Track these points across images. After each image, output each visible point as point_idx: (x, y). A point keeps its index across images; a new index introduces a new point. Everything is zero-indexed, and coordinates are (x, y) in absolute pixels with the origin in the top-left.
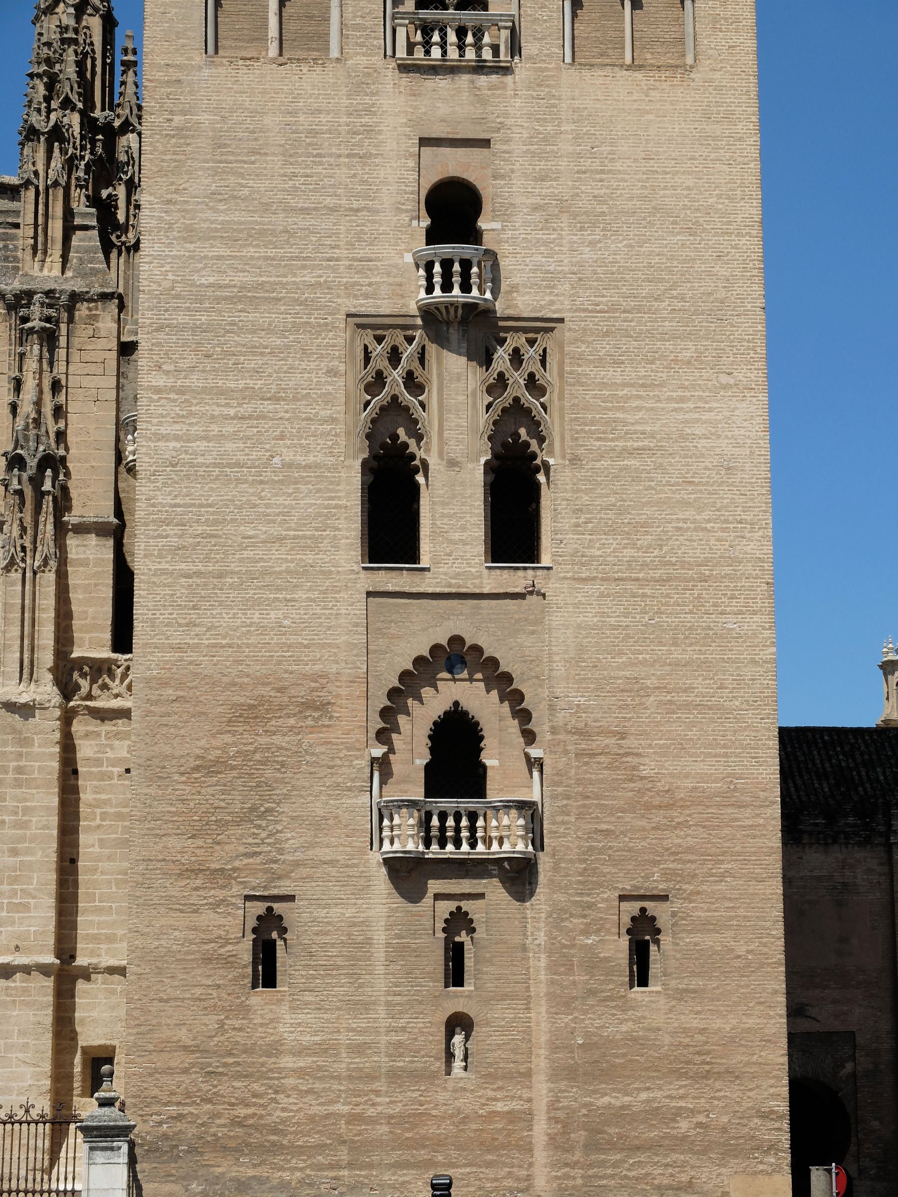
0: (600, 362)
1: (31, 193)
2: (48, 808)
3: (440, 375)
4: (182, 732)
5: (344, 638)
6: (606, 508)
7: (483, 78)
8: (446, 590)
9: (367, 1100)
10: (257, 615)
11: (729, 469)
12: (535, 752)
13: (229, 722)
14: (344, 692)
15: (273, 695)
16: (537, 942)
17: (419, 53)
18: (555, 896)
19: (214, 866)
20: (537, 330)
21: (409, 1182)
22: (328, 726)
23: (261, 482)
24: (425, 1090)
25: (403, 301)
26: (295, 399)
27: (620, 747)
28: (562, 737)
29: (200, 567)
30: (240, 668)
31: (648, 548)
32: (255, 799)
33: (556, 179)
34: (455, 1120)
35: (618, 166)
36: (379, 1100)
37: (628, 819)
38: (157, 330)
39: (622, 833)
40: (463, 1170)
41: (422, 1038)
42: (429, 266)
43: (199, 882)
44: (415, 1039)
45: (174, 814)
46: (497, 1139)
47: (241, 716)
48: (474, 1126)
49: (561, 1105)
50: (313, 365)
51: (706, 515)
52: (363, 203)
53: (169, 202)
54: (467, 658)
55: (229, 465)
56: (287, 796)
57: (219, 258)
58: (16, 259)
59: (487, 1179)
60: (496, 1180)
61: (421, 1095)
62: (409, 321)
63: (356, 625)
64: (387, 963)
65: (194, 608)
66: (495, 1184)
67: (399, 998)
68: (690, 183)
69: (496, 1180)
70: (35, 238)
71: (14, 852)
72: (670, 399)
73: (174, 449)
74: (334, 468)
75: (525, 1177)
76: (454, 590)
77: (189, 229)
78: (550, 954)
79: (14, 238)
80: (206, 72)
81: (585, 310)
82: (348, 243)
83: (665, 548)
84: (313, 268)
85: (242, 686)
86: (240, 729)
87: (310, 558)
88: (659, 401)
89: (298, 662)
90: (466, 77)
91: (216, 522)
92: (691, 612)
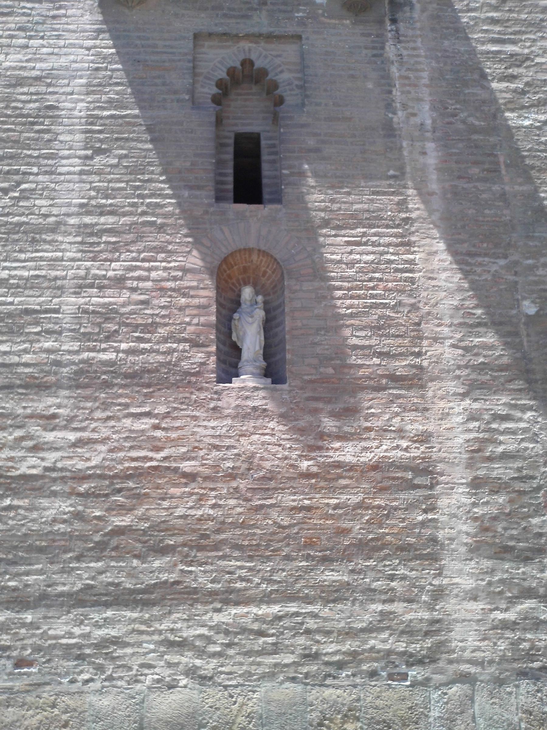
9: (22, 438)
16: (417, 120)
18: (446, 43)
21: (116, 642)
24: (167, 415)
34: (242, 484)
36: (50, 436)
40: (264, 610)
41: (163, 301)
44: (145, 303)
46: (345, 532)
48: (289, 500)
49: (500, 449)
59: (328, 633)
60: (350, 633)
61: (156, 427)
64: (89, 152)
66: (349, 645)
67: (111, 219)
69: (350, 633)
75: (424, 627)
78: (445, 140)
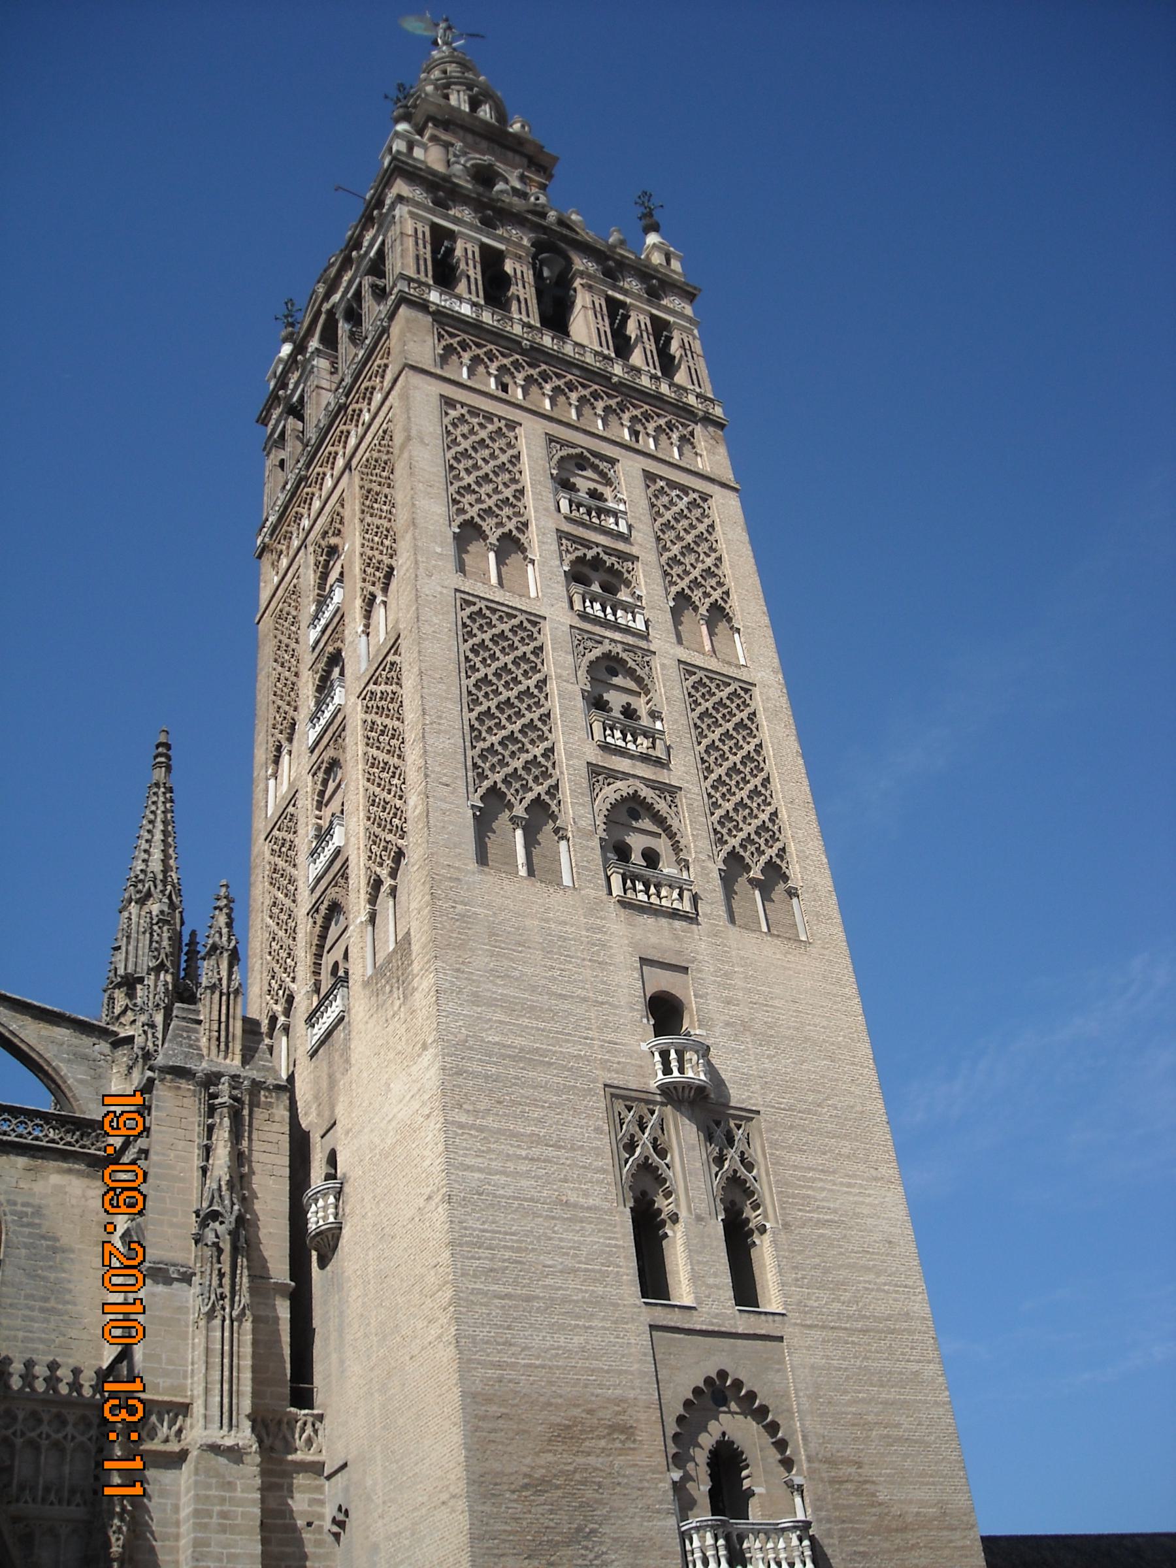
0: (790, 1149)
1: (217, 995)
2: (251, 1556)
3: (679, 1144)
4: (509, 1449)
5: (636, 1366)
6: (815, 1267)
7: (677, 922)
8: (710, 1328)
10: (562, 1340)
11: (890, 1242)
12: (798, 1480)
13: (550, 1440)
14: (643, 1416)
15: (584, 1415)
17: (630, 894)
20: (741, 1118)
22: (634, 1449)
23: (553, 1218)
25: (643, 1080)
26: (573, 1149)
27: (860, 1475)
28: (816, 1465)
30: (554, 1389)
31: (848, 1303)
32: (579, 1520)
33: (738, 1005)
35: (776, 1003)
37: (876, 1542)
38: (456, 1073)
39: (876, 1554)
42: (665, 1055)
45: (510, 1533)
47: (559, 1436)
50: (583, 1122)
51: (882, 1279)
52: (605, 999)
53: (458, 970)
54: (728, 1393)
55: (525, 1200)
56: (606, 1518)
57: (501, 1022)
58: (199, 1048)
62: (651, 1097)
63: (645, 1355)
65: (509, 1328)
68: (825, 1023)
70: (219, 1031)
72: (841, 1184)
73: (479, 1179)
74: (609, 1212)
76: (716, 1329)
77: (475, 995)
79: (196, 1031)
80: (478, 877)
81: (773, 1107)
82: (598, 1027)
83: (860, 1304)
84: (575, 1042)
85: (557, 1406)
86: (560, 1449)
87: (600, 1290)
88: (834, 1184)
89: (600, 1386)
90: (664, 922)
91: (519, 1250)
92: (887, 1359)
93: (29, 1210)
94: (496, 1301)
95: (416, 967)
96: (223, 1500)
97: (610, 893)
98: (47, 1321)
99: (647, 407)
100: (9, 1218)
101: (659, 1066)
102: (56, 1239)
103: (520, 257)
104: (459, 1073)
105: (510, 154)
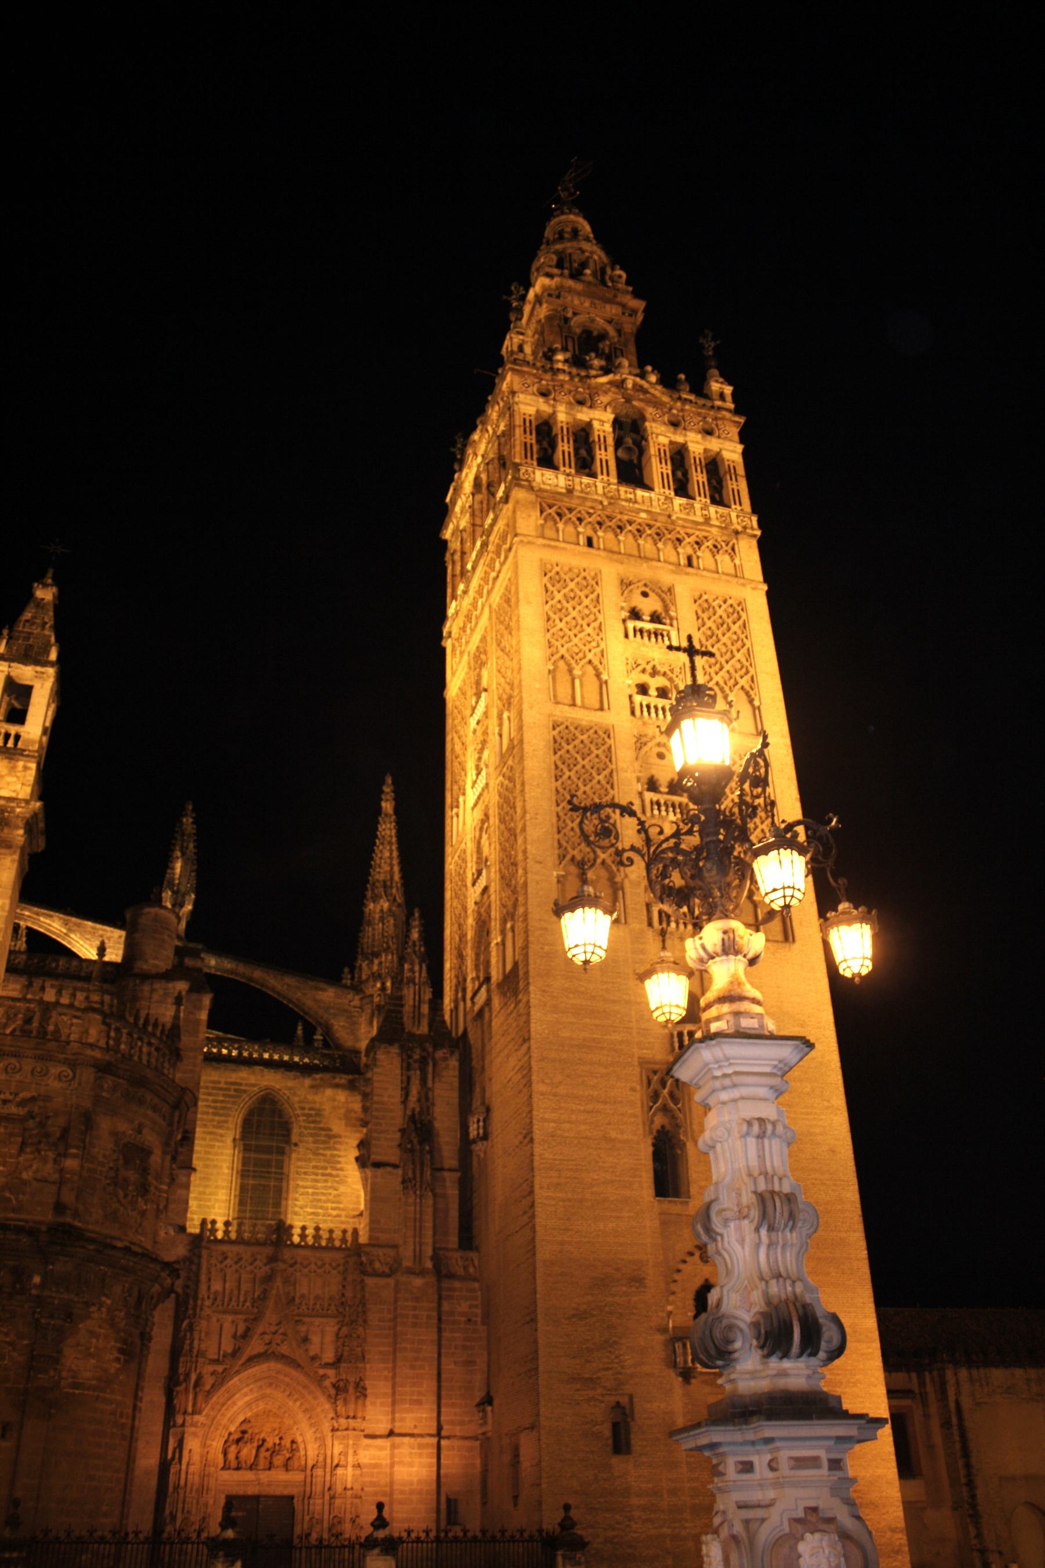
11: (834, 1151)
19: (586, 1376)
29: (570, 1196)
43: (578, 1386)
57: (571, 1023)
58: (402, 1024)
65: (568, 1219)
71: (413, 1367)
72: (802, 1113)
79: (401, 1012)
93: (313, 1112)
94: (561, 1203)
95: (521, 984)
96: (415, 1308)
97: (650, 924)
98: (326, 1181)
99: (697, 533)
100: (301, 1118)
101: (677, 1045)
102: (330, 1130)
103: (602, 422)
104: (542, 1059)
105: (608, 307)
